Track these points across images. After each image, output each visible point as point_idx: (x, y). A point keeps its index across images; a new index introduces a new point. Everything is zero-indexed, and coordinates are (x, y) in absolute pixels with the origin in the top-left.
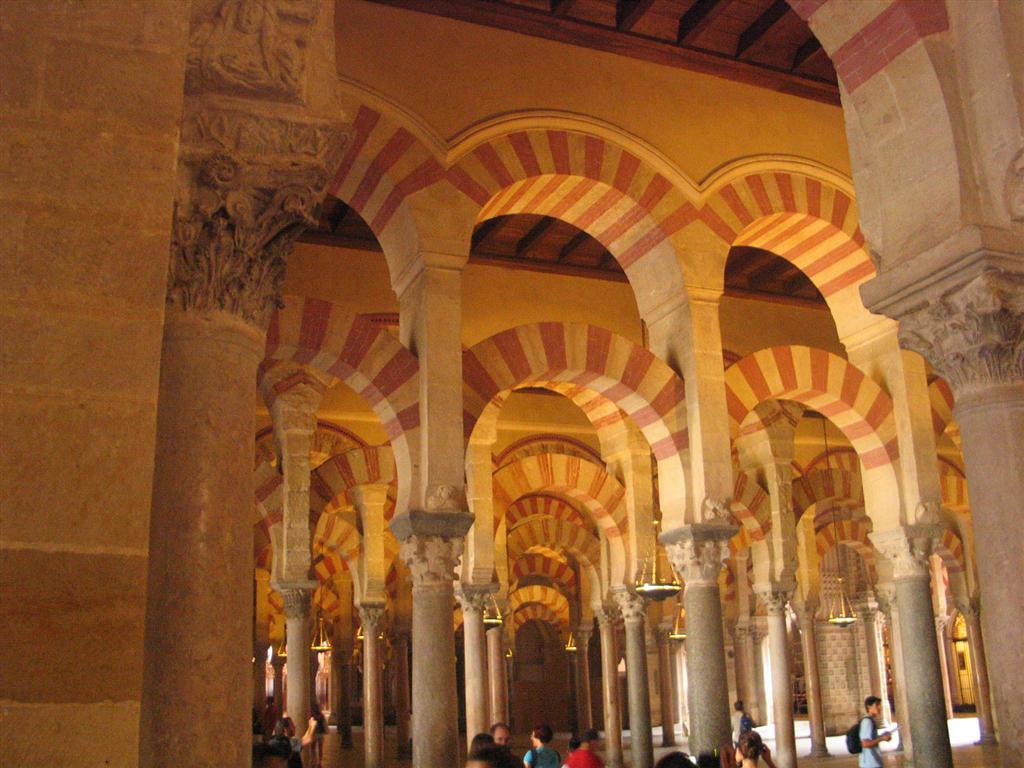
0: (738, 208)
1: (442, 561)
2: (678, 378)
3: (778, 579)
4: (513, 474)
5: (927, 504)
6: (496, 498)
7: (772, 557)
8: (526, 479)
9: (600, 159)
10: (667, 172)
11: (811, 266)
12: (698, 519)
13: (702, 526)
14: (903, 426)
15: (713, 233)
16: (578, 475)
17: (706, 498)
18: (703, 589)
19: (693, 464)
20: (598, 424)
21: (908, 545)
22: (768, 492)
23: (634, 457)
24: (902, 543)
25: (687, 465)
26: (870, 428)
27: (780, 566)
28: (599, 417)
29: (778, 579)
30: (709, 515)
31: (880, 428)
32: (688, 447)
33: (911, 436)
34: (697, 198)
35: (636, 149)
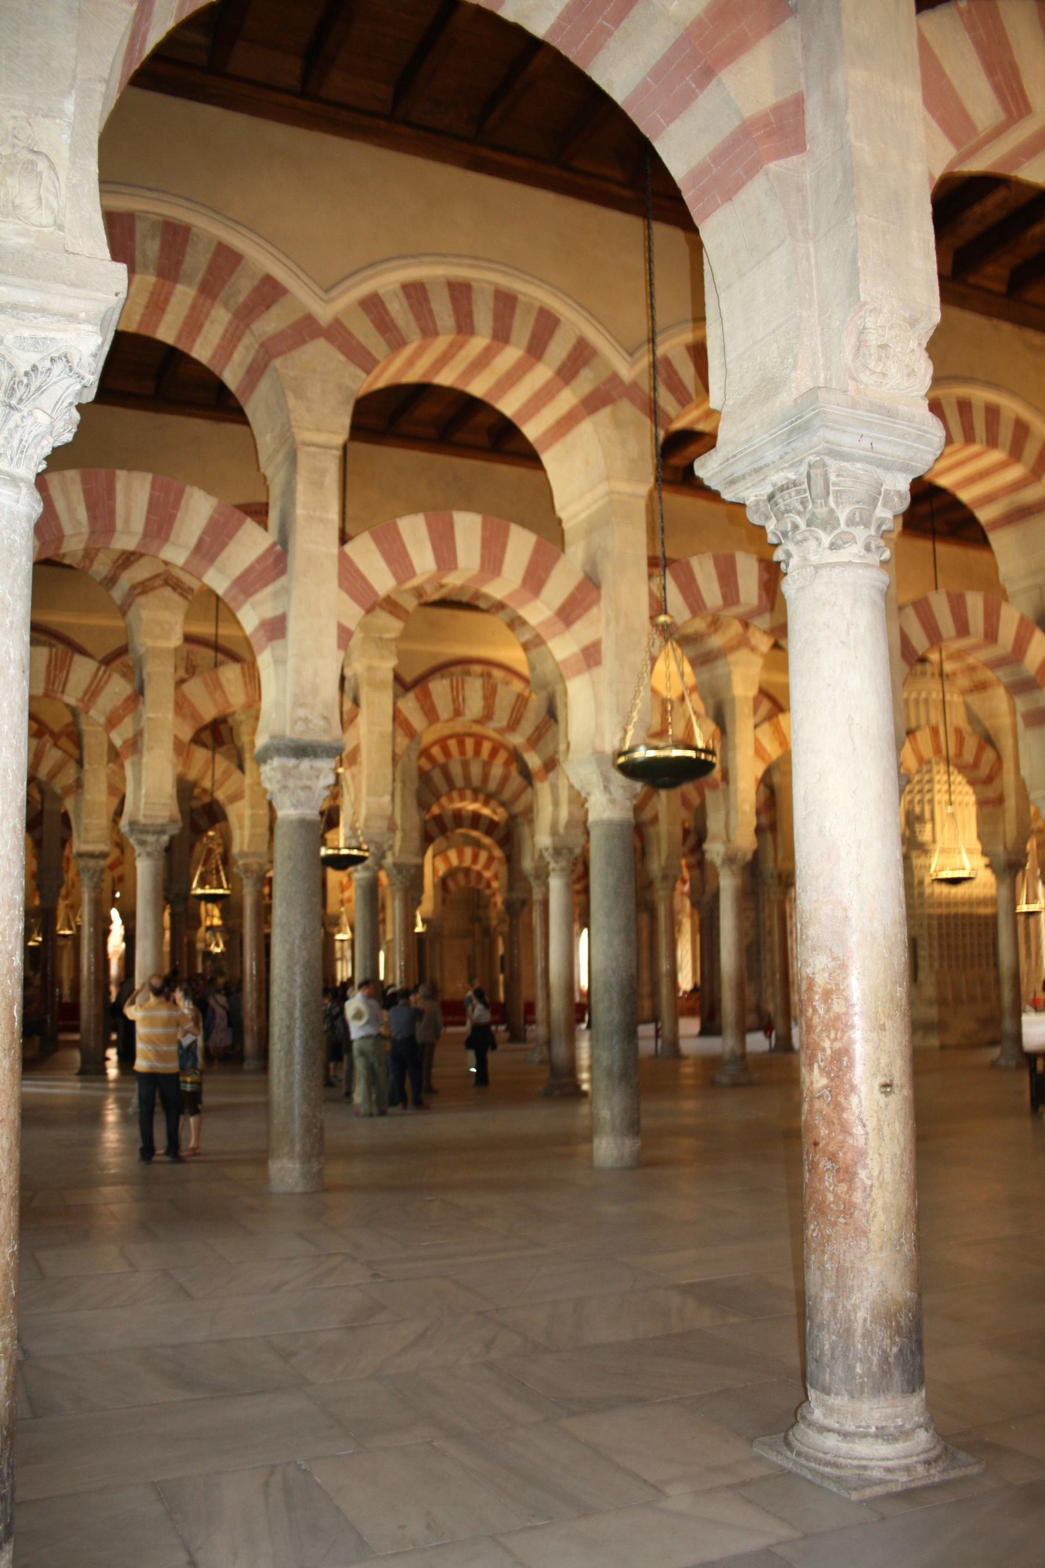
0: (383, 323)
2: (278, 548)
3: (561, 830)
4: (207, 686)
7: (556, 803)
8: (224, 693)
9: (182, 253)
10: (281, 274)
11: (519, 412)
13: (292, 741)
15: (342, 357)
18: (291, 822)
22: (556, 720)
23: (371, 669)
26: (561, 625)
27: (564, 814)
29: (561, 830)
30: (300, 726)
31: (578, 626)
34: (324, 313)
35: (238, 242)
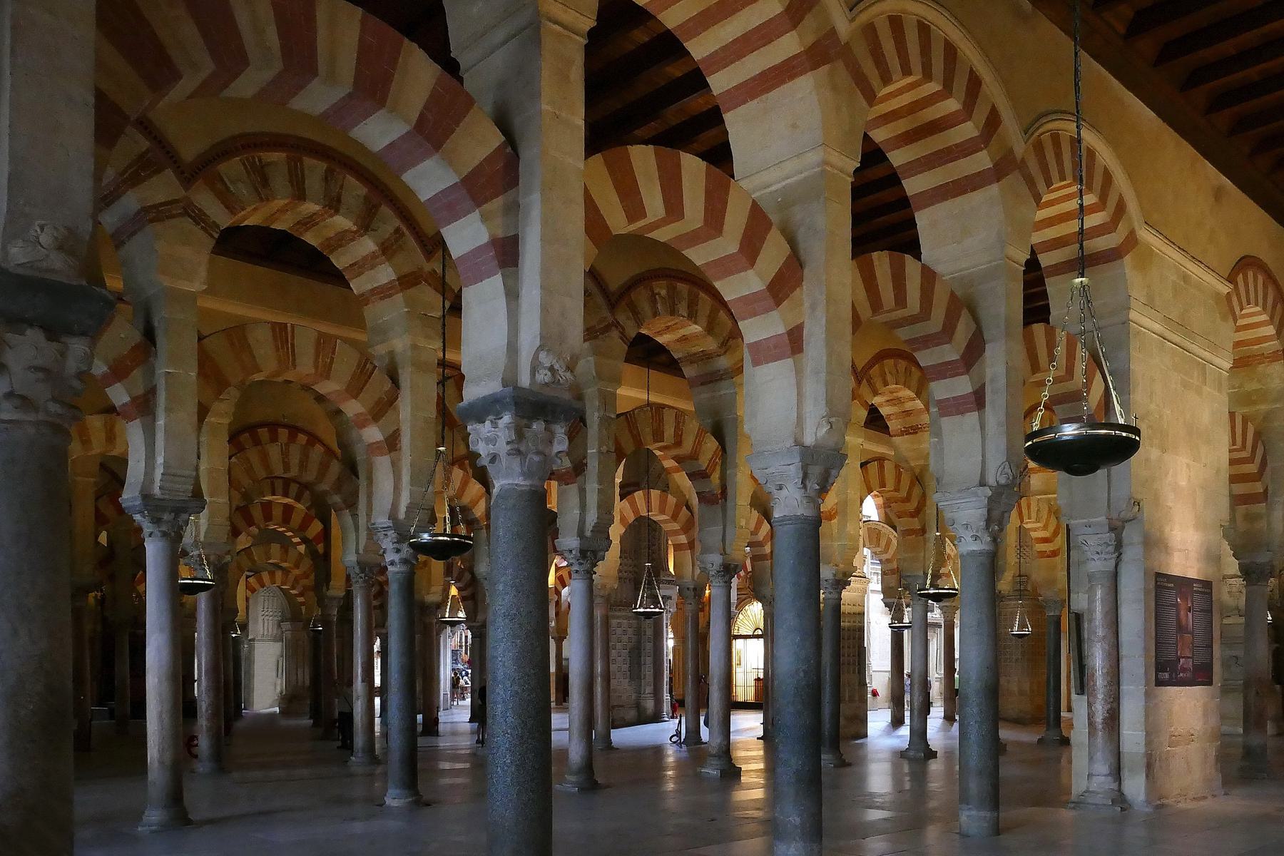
1: (41, 375)
5: (833, 420)
6: (202, 373)
12: (525, 380)
13: (530, 391)
14: (813, 308)
16: (332, 362)
17: (541, 348)
19: (524, 292)
20: (364, 299)
21: (801, 475)
24: (794, 471)
25: (512, 295)
26: (771, 302)
28: (370, 287)
32: (517, 266)
33: (824, 321)
